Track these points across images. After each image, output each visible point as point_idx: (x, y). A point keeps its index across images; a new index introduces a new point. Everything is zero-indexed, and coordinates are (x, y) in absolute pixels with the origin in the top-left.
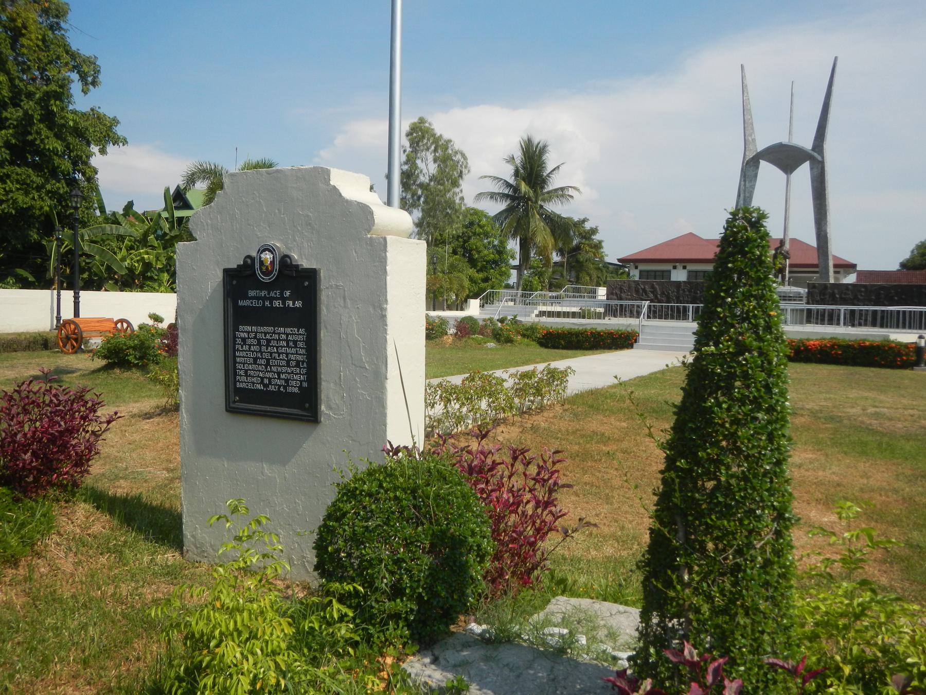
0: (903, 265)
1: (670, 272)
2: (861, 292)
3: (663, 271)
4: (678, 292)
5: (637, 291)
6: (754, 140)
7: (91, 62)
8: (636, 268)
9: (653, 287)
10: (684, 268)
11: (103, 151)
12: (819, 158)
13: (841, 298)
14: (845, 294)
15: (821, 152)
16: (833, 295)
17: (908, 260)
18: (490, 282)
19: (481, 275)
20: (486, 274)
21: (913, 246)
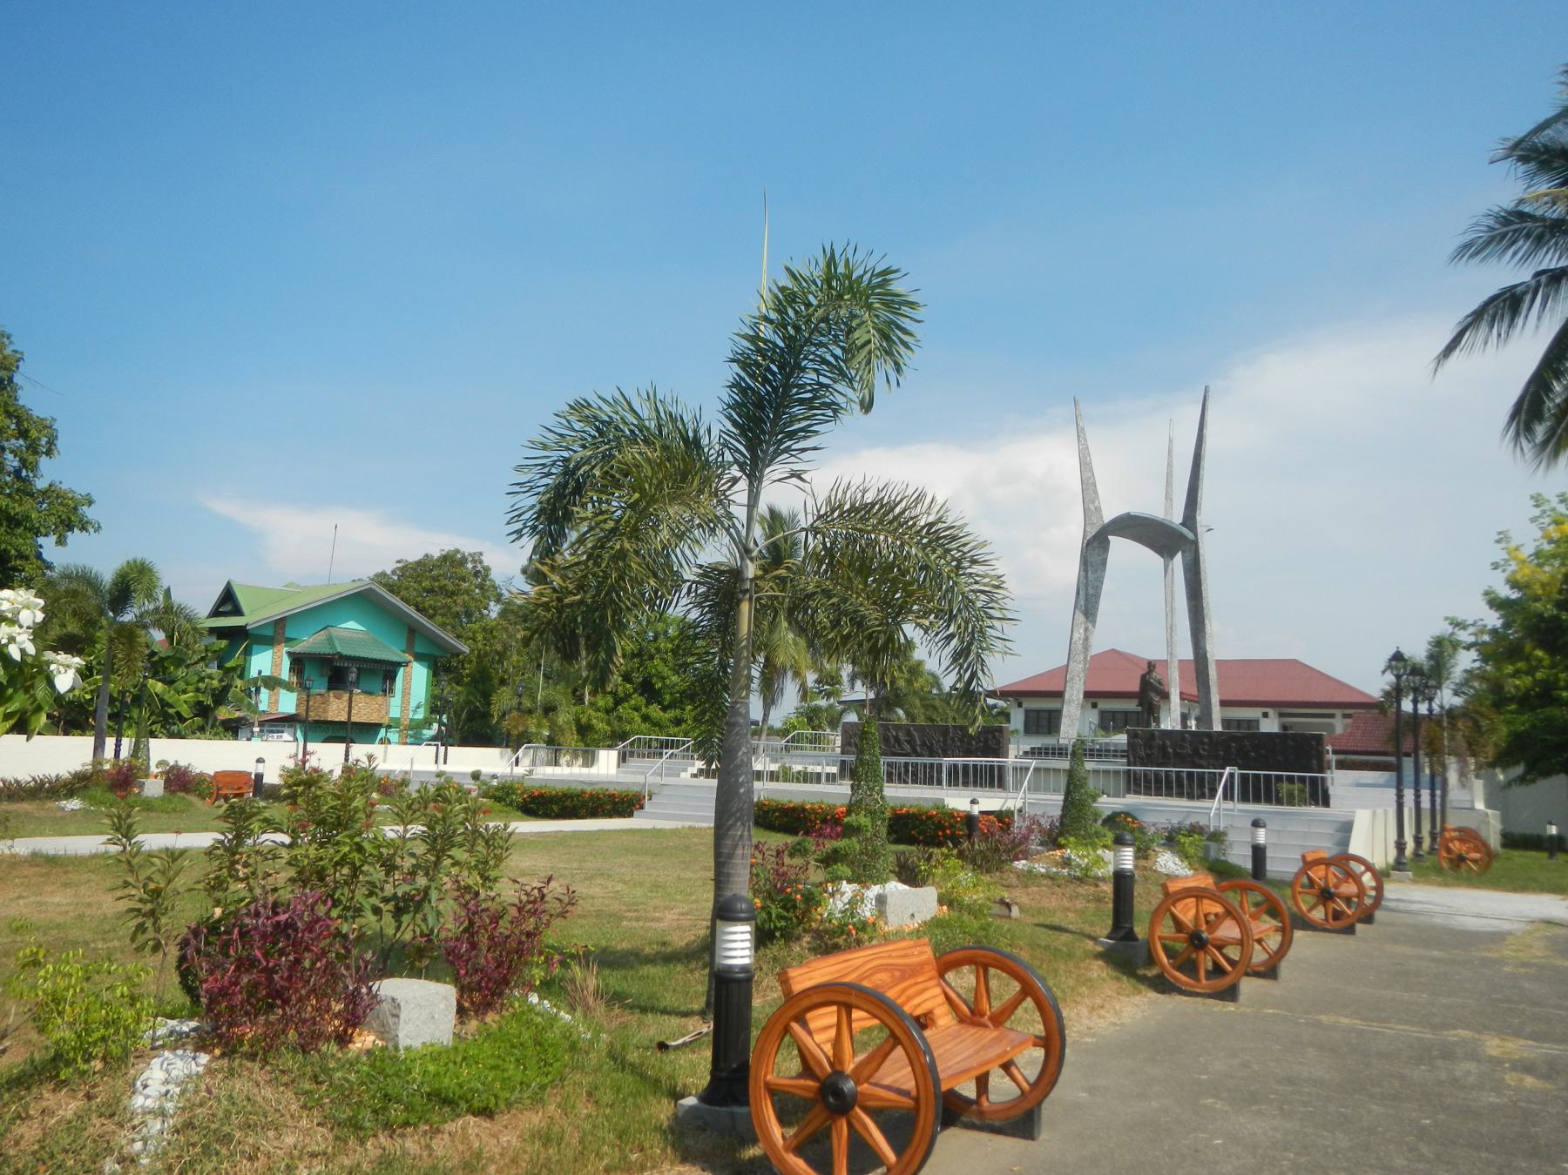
2: (1203, 743)
4: (945, 742)
6: (1098, 509)
7: (46, 426)
8: (1020, 705)
9: (909, 733)
11: (61, 541)
12: (1190, 536)
13: (1176, 754)
14: (1182, 747)
15: (1194, 529)
16: (1163, 748)
19: (671, 714)
20: (678, 711)
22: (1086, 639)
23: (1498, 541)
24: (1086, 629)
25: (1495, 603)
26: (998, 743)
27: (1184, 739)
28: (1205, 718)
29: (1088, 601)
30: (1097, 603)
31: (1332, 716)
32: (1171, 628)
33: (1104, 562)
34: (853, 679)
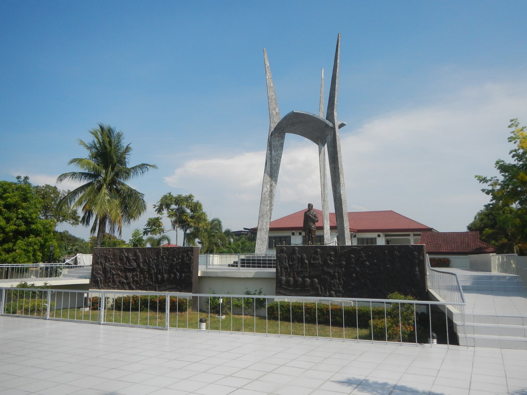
0: (469, 228)
1: (290, 237)
2: (331, 255)
3: (285, 237)
4: (157, 260)
5: (121, 260)
9: (135, 254)
10: (300, 234)
12: (331, 124)
14: (314, 259)
16: (302, 260)
17: (471, 224)
18: (14, 253)
19: (6, 246)
20: (11, 245)
21: (475, 214)
22: (271, 191)
23: (509, 127)
24: (271, 186)
25: (503, 168)
26: (190, 259)
27: (316, 253)
28: (341, 237)
29: (272, 169)
30: (278, 169)
31: (409, 235)
32: (323, 185)
33: (282, 145)
34: (174, 224)
